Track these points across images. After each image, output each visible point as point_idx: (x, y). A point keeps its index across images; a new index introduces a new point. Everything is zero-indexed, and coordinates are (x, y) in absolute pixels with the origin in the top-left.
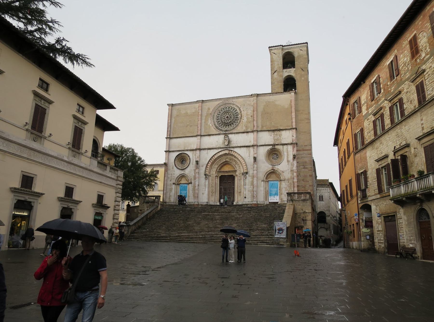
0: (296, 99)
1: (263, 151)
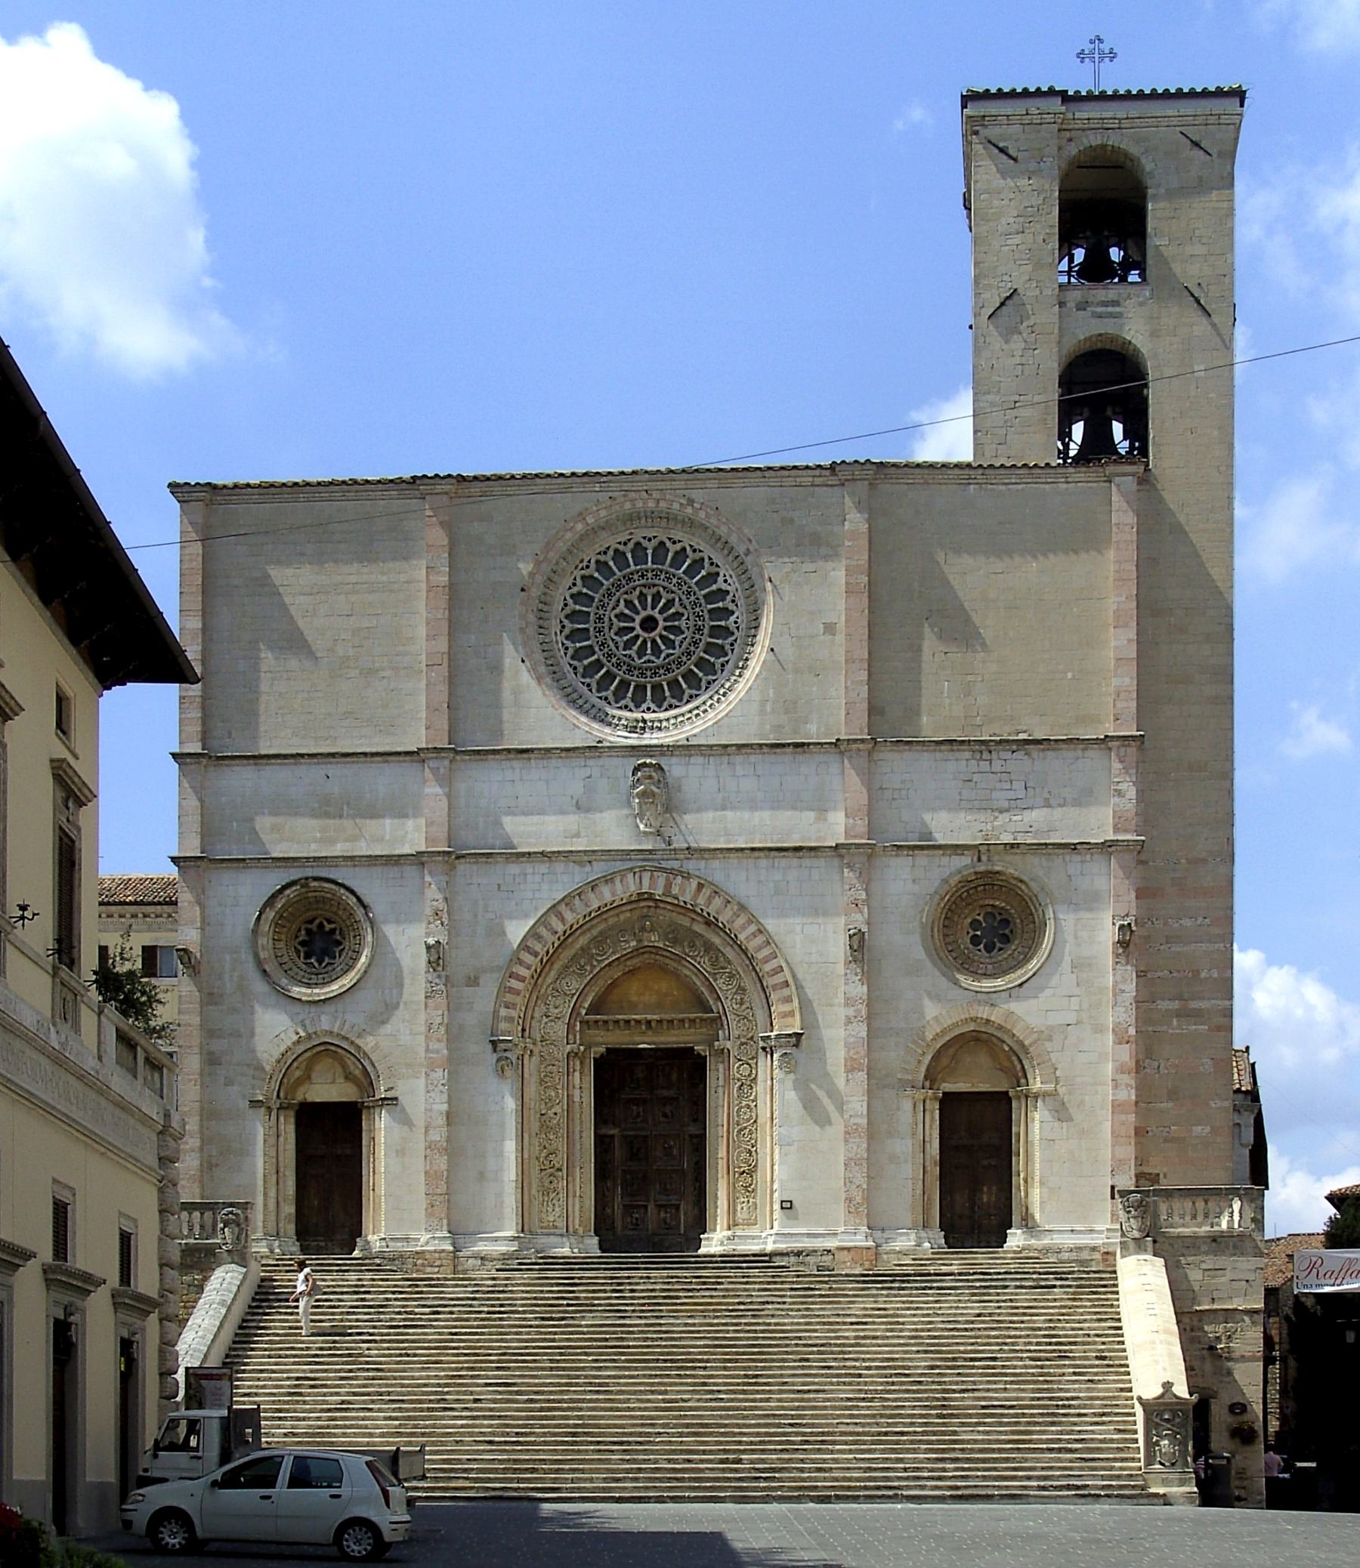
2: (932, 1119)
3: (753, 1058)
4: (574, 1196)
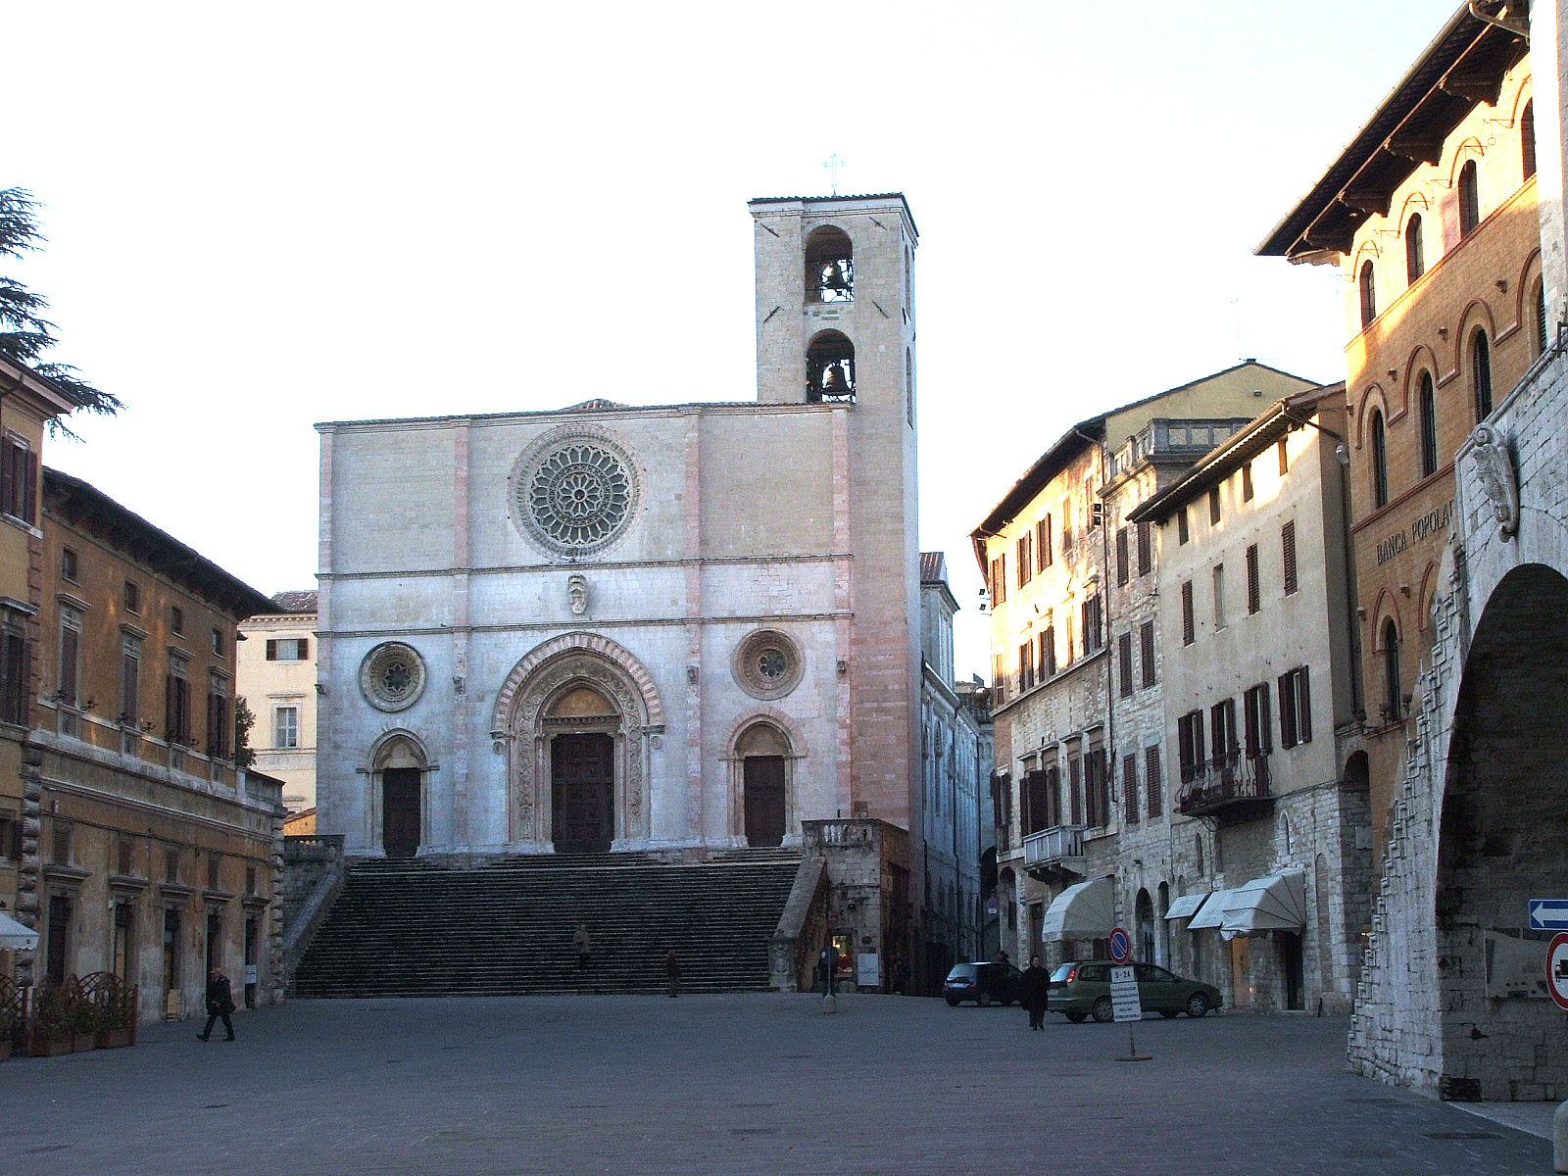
0: (856, 436)
1: (724, 641)
2: (739, 773)
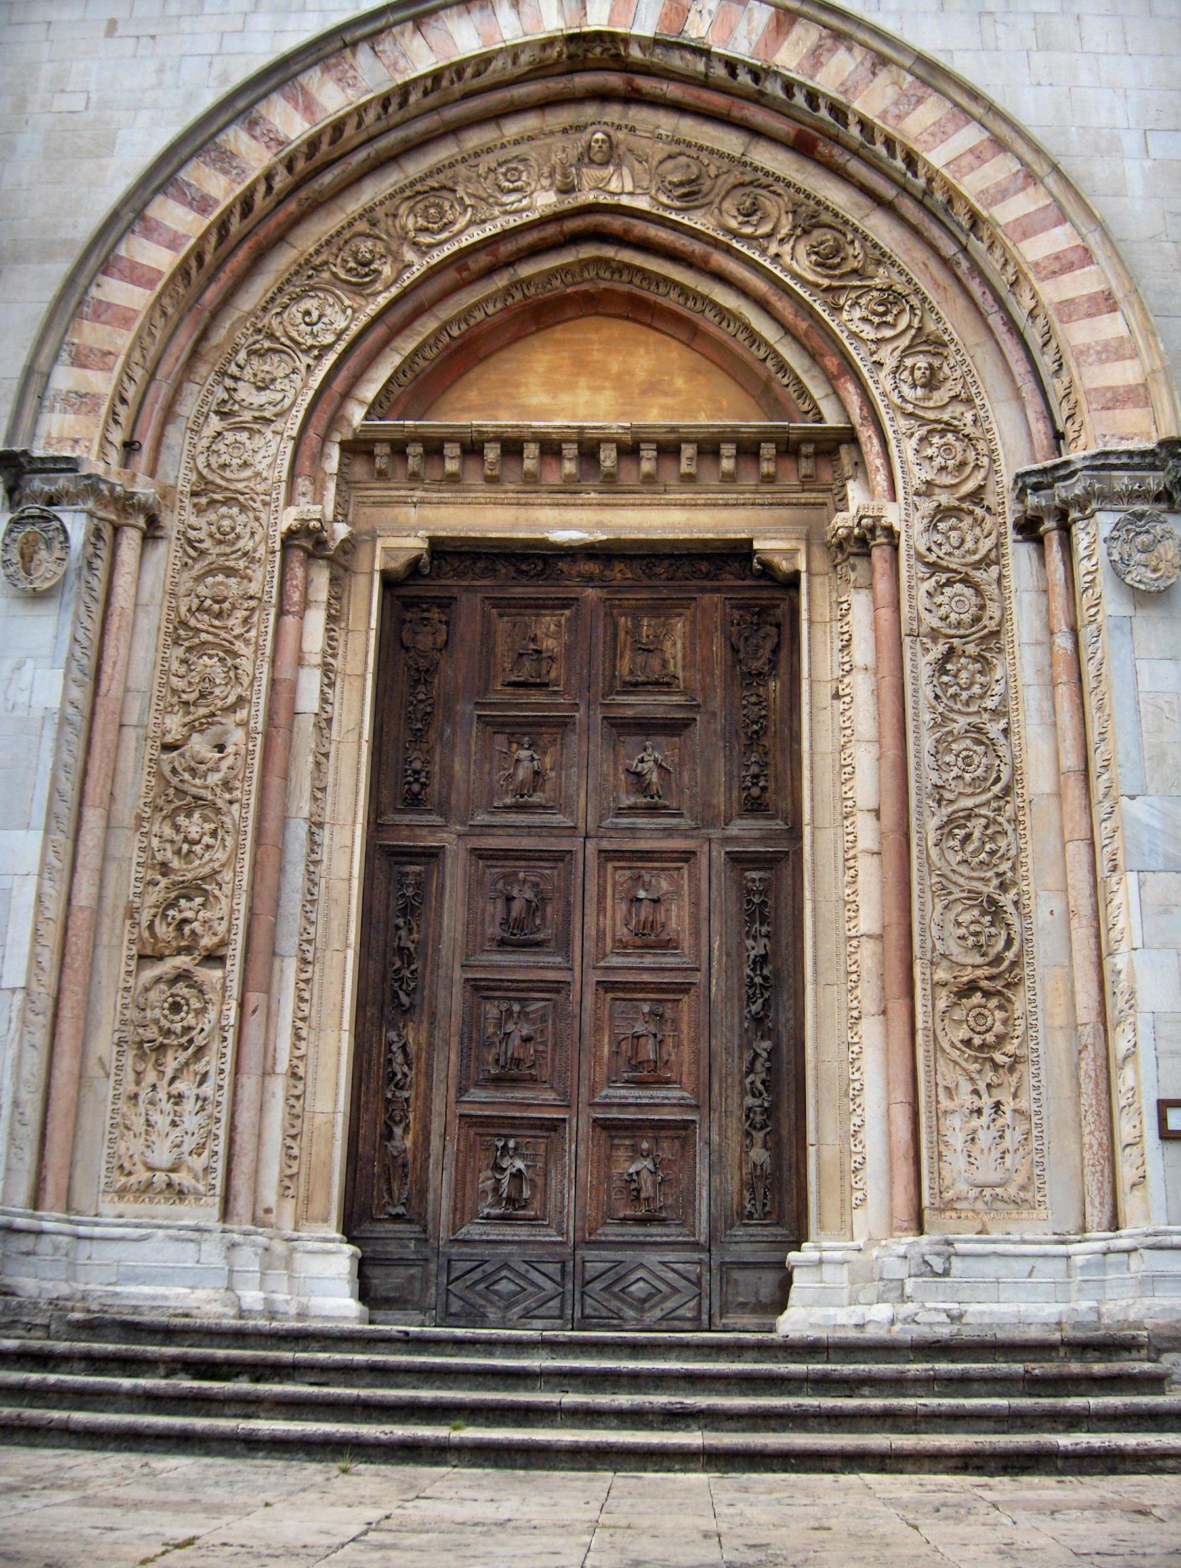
3: (985, 562)
4: (267, 1072)
